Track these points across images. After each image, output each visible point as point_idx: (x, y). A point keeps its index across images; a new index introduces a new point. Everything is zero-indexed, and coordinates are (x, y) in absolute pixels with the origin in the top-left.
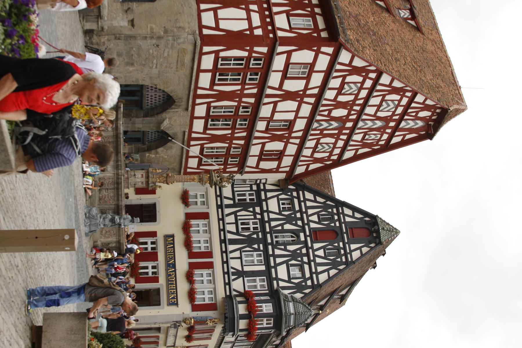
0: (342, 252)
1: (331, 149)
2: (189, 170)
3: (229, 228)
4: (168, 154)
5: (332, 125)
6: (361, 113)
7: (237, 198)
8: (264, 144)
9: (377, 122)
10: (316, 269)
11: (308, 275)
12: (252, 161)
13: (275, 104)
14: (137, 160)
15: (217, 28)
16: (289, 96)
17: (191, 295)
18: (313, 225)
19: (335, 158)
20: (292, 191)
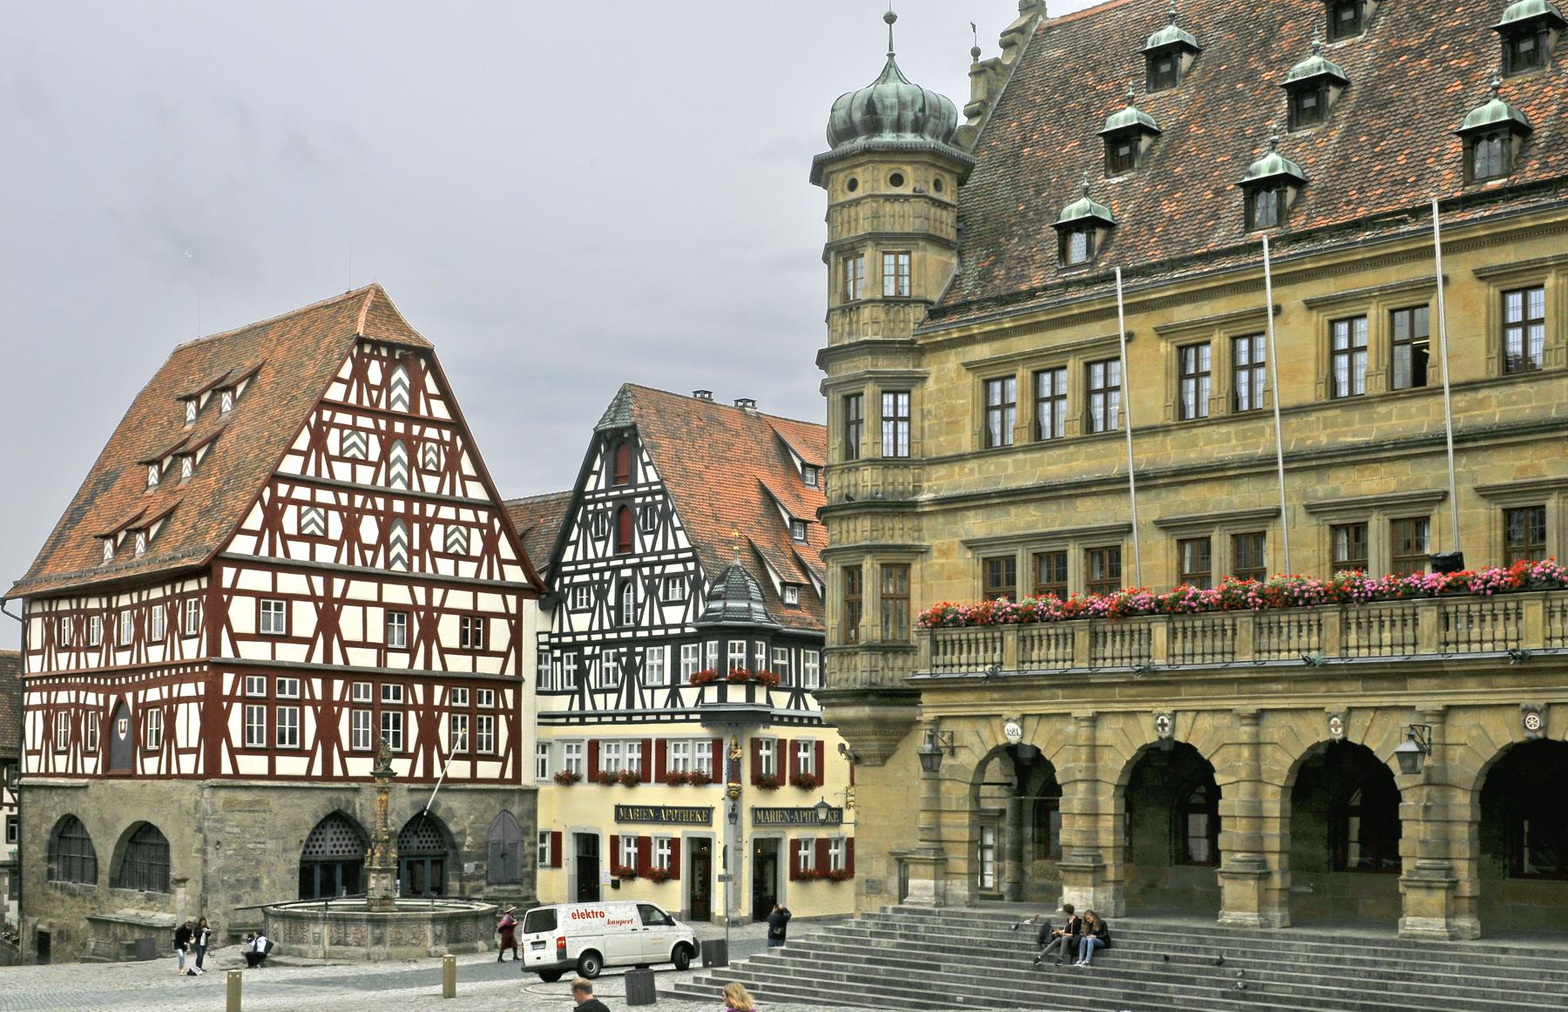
0: (649, 499)
1: (463, 529)
2: (509, 775)
3: (611, 707)
4: (461, 815)
5: (398, 539)
6: (369, 493)
7: (573, 687)
8: (443, 651)
9: (393, 457)
10: (671, 552)
11: (679, 568)
12: (489, 666)
13: (344, 645)
14: (477, 867)
15: (196, 751)
16: (328, 623)
17: (699, 780)
18: (610, 553)
19: (483, 516)
20: (562, 586)
